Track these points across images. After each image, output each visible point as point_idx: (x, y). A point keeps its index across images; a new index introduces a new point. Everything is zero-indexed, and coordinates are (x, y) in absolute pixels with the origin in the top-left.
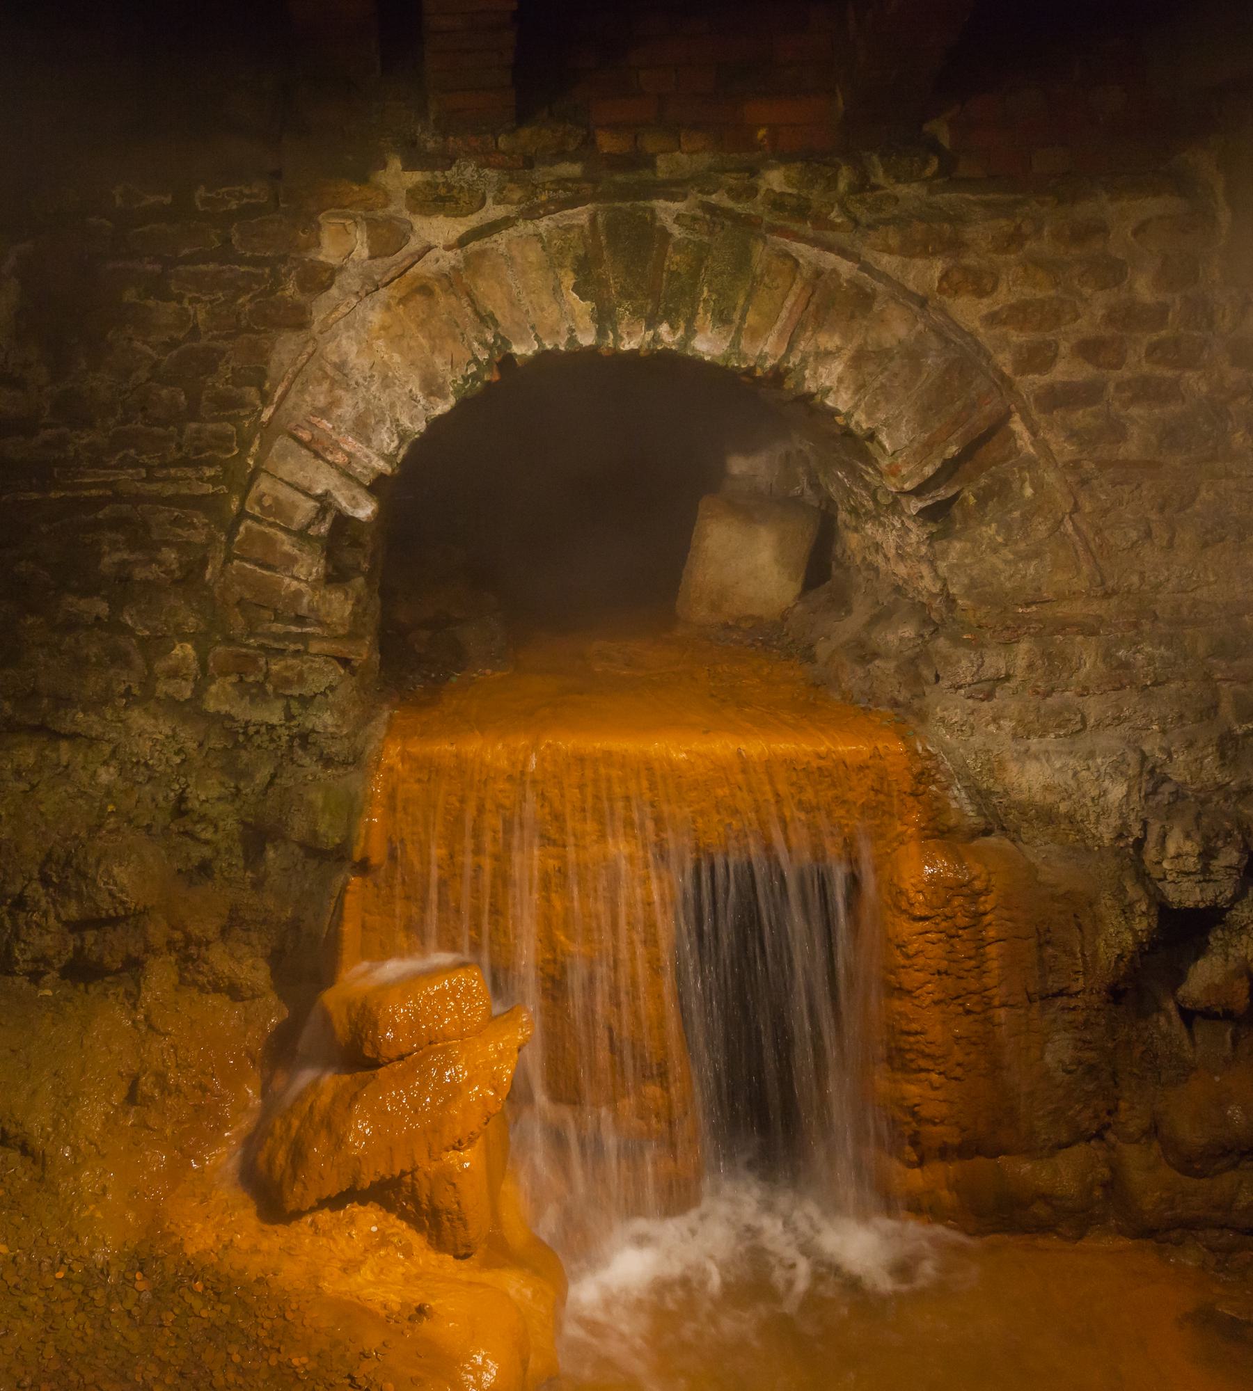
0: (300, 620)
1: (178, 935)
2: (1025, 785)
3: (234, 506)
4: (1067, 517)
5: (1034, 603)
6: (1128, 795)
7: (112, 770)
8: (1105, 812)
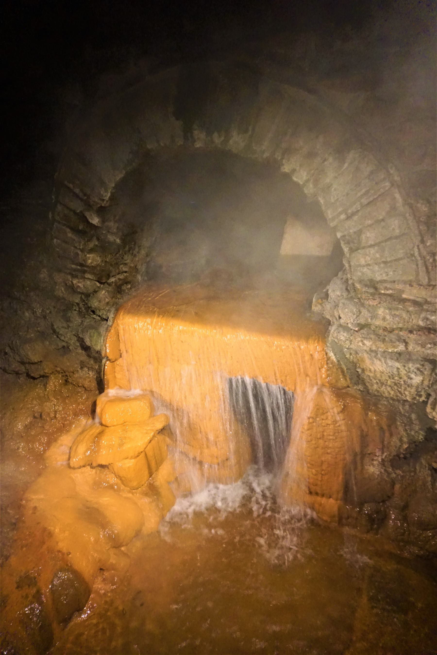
0: (81, 265)
1: (59, 369)
2: (373, 369)
3: (50, 216)
4: (416, 247)
5: (391, 289)
6: (423, 381)
7: (30, 312)
8: (410, 386)
